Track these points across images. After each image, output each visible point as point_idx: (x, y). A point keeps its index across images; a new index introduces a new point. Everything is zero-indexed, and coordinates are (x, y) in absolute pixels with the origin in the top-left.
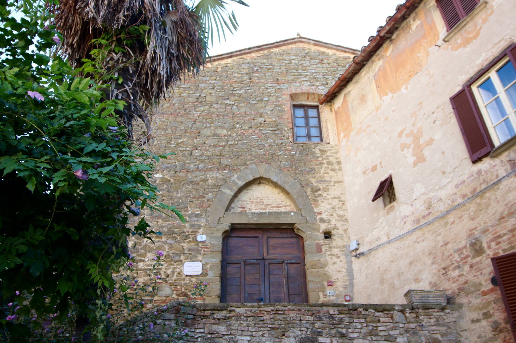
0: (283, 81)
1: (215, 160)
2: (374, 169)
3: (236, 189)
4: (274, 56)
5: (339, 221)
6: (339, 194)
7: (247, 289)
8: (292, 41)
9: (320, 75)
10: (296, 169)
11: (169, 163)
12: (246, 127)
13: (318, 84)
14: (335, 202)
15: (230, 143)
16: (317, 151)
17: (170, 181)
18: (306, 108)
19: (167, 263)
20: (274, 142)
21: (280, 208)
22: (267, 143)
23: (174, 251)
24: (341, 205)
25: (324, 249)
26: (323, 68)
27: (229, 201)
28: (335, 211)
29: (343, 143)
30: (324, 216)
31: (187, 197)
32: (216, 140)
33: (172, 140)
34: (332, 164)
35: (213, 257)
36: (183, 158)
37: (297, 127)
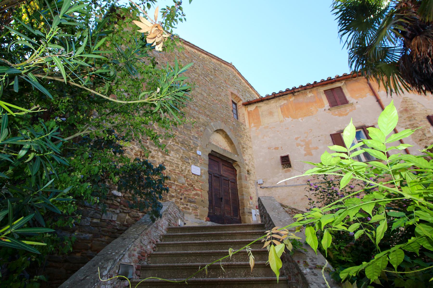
23: (186, 156)
30: (247, 162)
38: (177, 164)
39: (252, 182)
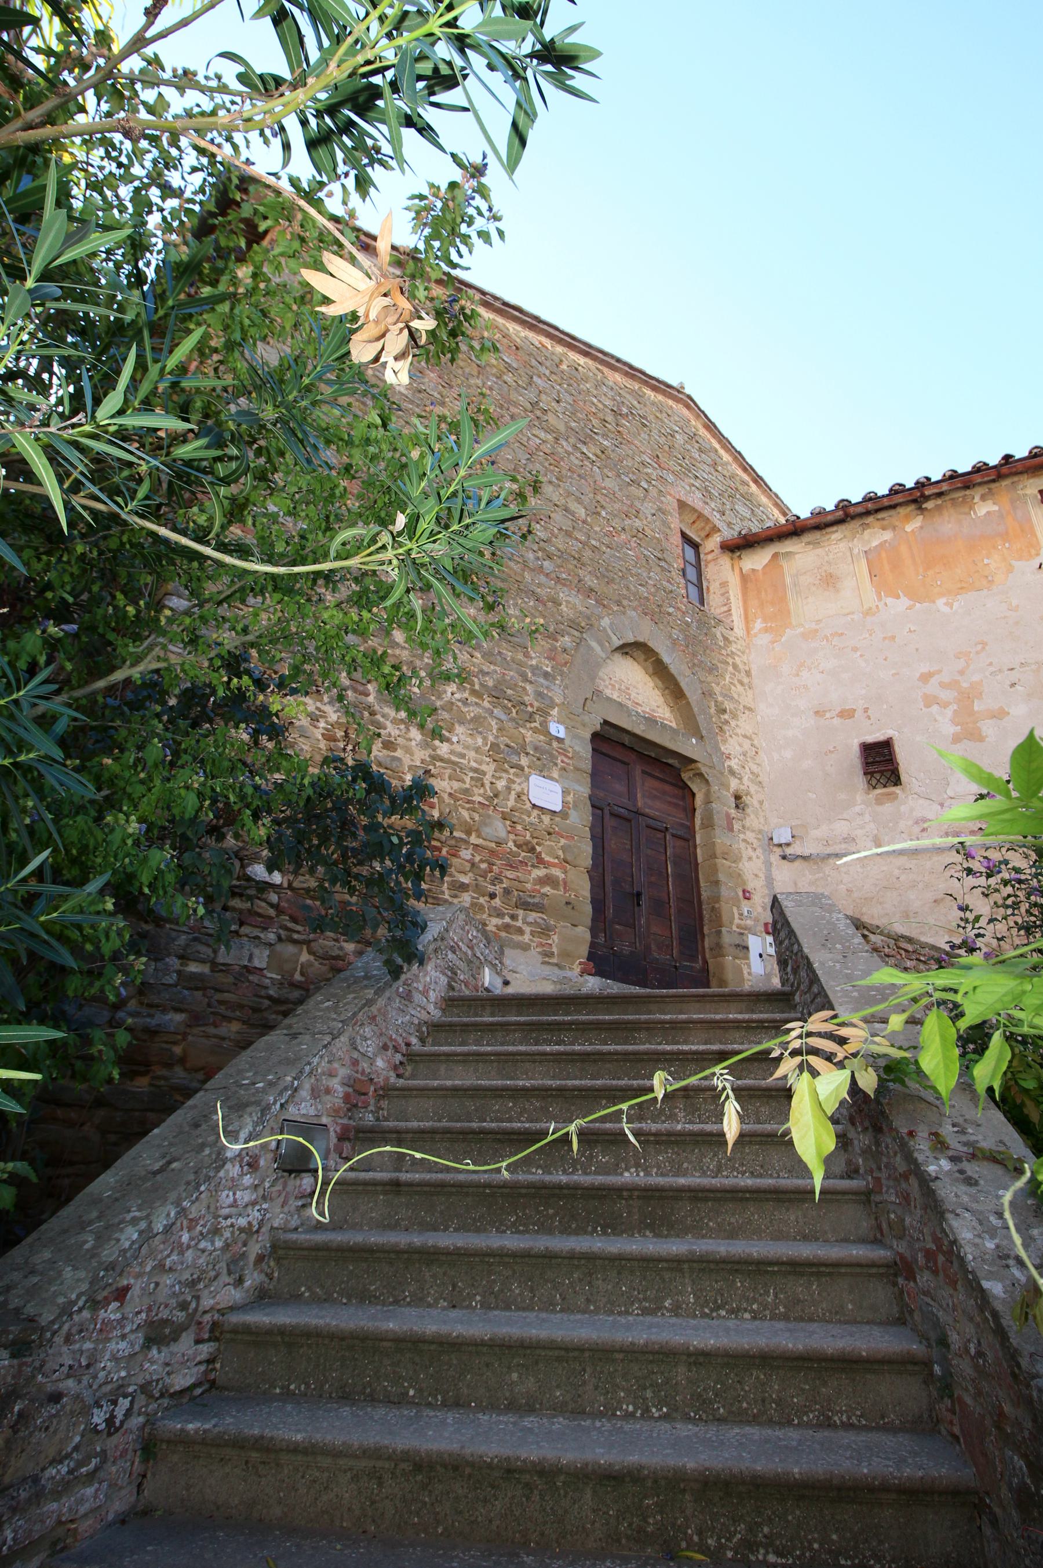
30: (733, 763)
38: (476, 770)
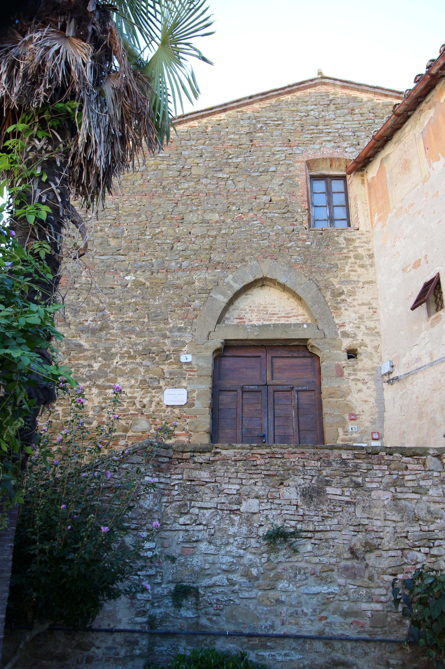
0: (297, 142)
1: (203, 256)
2: (417, 264)
3: (230, 294)
4: (284, 106)
5: (367, 335)
6: (369, 298)
7: (245, 423)
8: (310, 83)
9: (348, 131)
10: (311, 266)
11: (143, 261)
12: (244, 209)
13: (345, 145)
14: (364, 310)
15: (223, 232)
16: (341, 240)
17: (144, 284)
18: (329, 180)
19: (143, 390)
20: (282, 229)
21: (289, 319)
22: (272, 231)
23: (151, 375)
24: (372, 313)
25: (346, 372)
26: (353, 120)
27: (222, 309)
28: (364, 322)
29: (378, 229)
30: (348, 329)
31: (167, 305)
32: (205, 229)
33: (147, 229)
34: (362, 258)
35: (201, 383)
36: (160, 254)
37: (316, 206)
38: (130, 398)
39: (361, 375)
